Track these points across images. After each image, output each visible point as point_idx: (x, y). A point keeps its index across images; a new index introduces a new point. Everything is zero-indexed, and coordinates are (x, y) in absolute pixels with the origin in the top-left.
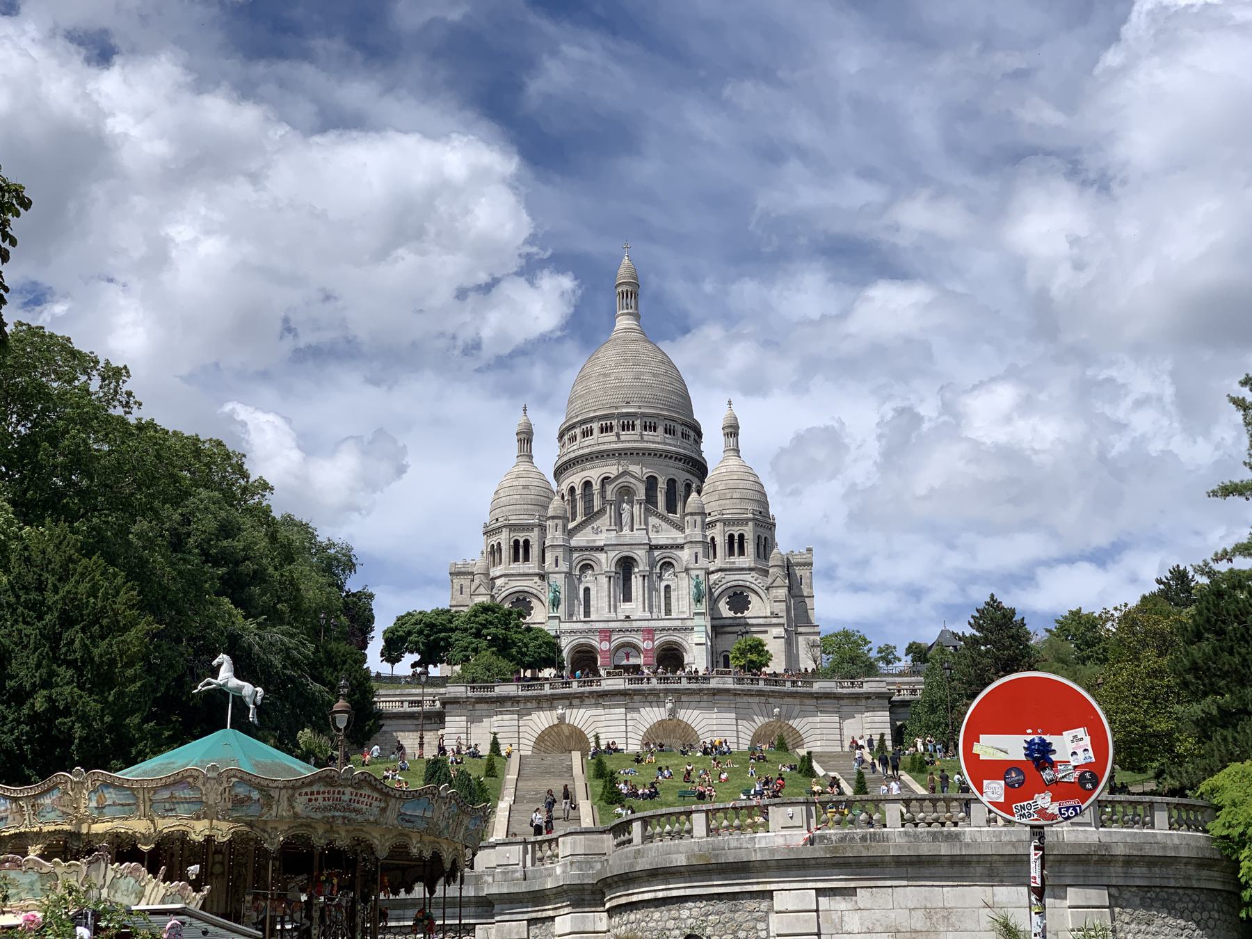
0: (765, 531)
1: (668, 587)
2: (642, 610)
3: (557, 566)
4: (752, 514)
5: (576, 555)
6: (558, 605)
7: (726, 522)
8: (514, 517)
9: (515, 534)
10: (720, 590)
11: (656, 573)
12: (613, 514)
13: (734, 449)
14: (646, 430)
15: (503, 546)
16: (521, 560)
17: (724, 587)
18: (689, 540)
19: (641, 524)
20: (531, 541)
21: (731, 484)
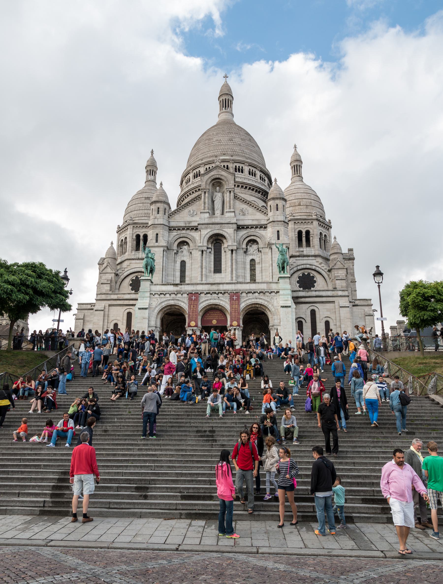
0: (324, 230)
1: (252, 261)
2: (230, 279)
3: (157, 241)
4: (316, 215)
5: (175, 233)
7: (296, 221)
8: (137, 218)
9: (137, 230)
10: (292, 271)
11: (243, 248)
12: (206, 200)
13: (299, 176)
14: (236, 172)
15: (128, 240)
16: (141, 249)
17: (295, 269)
18: (271, 220)
21: (299, 196)
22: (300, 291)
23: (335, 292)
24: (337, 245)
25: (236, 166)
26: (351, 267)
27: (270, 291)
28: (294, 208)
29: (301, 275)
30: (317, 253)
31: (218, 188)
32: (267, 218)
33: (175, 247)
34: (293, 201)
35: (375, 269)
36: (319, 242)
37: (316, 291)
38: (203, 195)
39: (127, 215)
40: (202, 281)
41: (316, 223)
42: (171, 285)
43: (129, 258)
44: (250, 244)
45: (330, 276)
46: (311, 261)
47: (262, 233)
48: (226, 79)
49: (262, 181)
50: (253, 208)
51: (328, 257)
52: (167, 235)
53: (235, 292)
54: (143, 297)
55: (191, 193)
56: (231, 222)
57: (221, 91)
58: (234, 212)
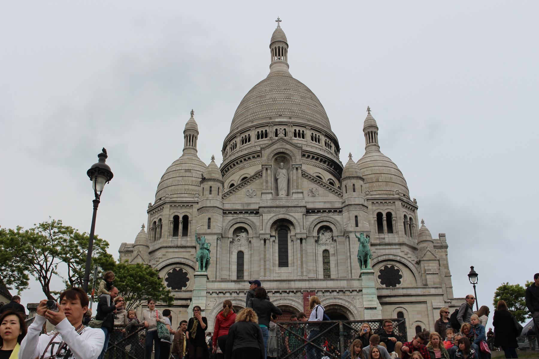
0: (409, 212)
1: (326, 251)
2: (299, 274)
3: (209, 227)
4: (398, 194)
5: (230, 217)
6: (207, 263)
7: (374, 201)
8: (175, 196)
9: (175, 211)
12: (269, 178)
13: (375, 145)
14: (295, 136)
15: (164, 222)
18: (347, 203)
19: (297, 188)
20: (190, 216)
22: (383, 288)
23: (427, 290)
24: (424, 231)
25: (295, 130)
26: (444, 257)
27: (351, 290)
28: (371, 185)
29: (383, 268)
30: (401, 241)
31: (282, 164)
32: (341, 201)
33: (230, 234)
34: (369, 176)
35: (470, 270)
36: (403, 227)
37: (403, 288)
38: (264, 171)
39: (162, 191)
40: (265, 276)
41: (398, 203)
42: (232, 281)
43: (165, 245)
44: (322, 231)
45: (419, 269)
46: (394, 251)
47: (337, 219)
48: (279, 24)
49: (327, 148)
50: (325, 187)
51: (416, 246)
52: (221, 220)
53: (309, 290)
54: (199, 297)
55: (239, 162)
56: (299, 205)
57: (272, 37)
58: (302, 193)
